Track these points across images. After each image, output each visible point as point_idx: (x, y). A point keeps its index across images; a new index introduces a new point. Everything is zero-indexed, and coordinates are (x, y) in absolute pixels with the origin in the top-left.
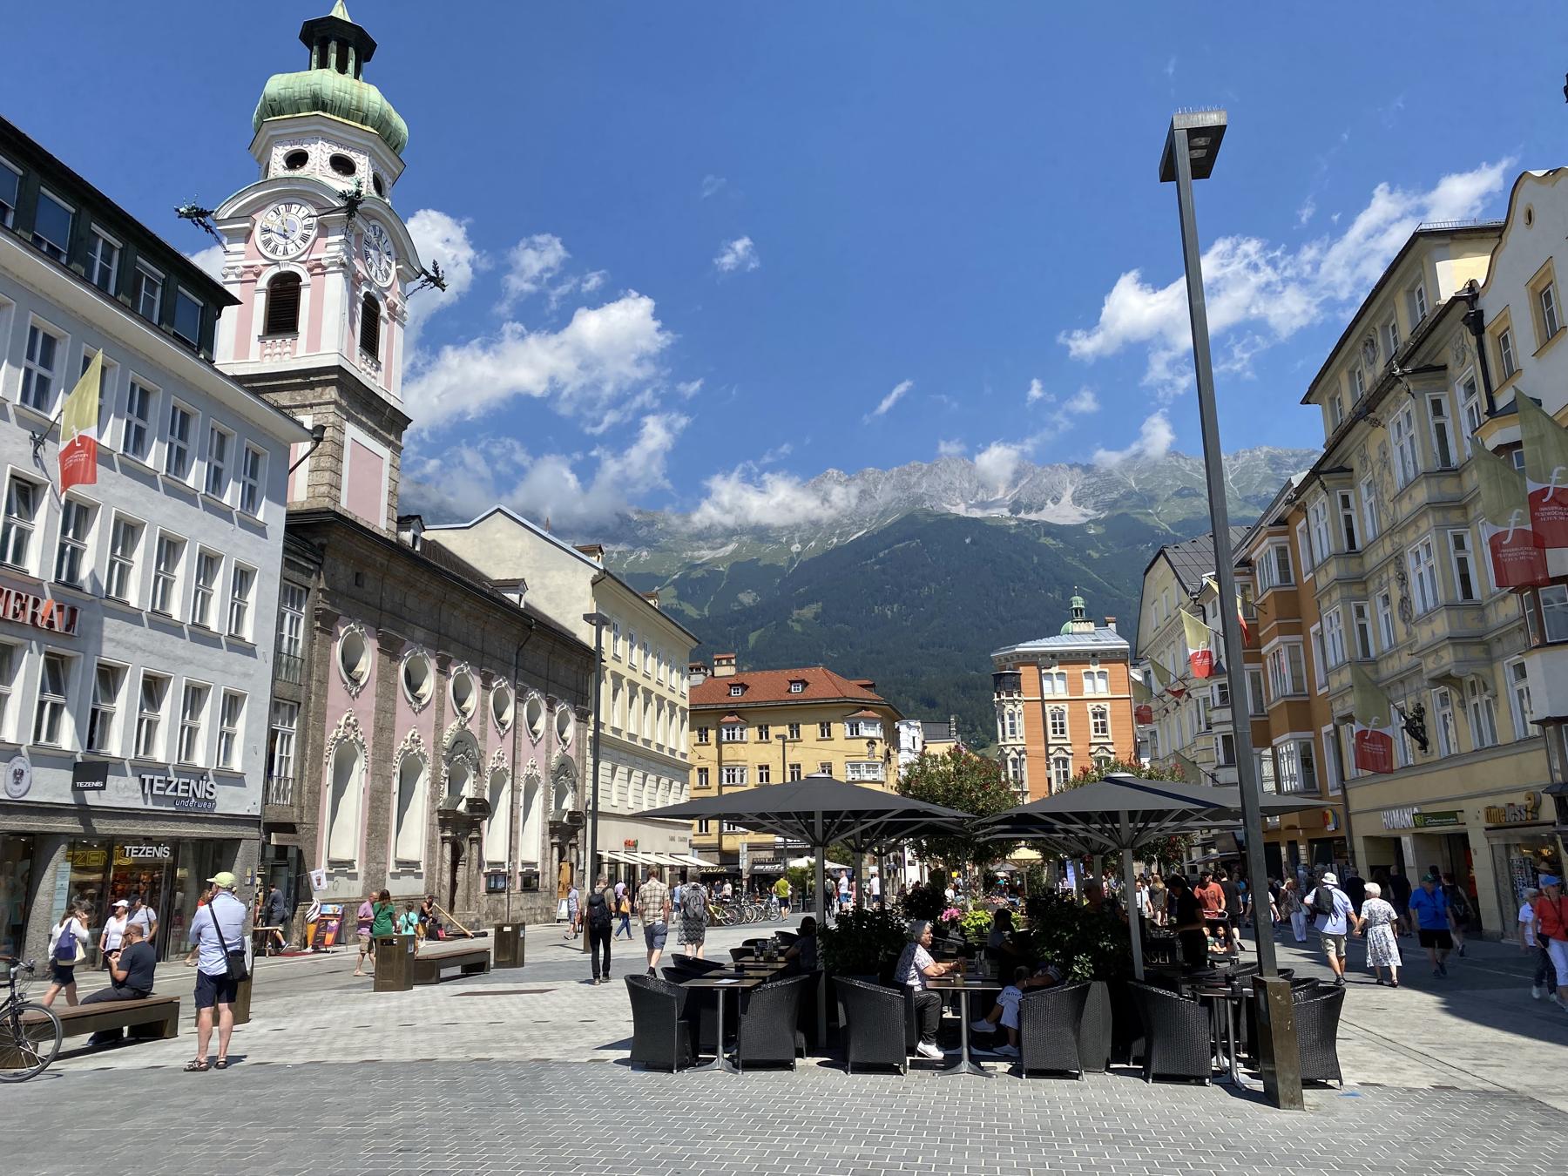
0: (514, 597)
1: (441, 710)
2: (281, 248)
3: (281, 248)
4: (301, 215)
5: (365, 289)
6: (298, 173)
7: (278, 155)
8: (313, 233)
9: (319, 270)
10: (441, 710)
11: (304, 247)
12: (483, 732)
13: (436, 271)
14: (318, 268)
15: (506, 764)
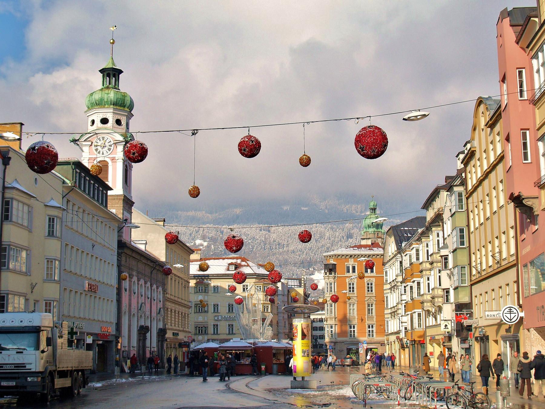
1: (138, 297)
2: (101, 152)
3: (101, 152)
4: (108, 141)
5: (125, 163)
6: (106, 126)
9: (114, 161)
10: (138, 297)
11: (109, 152)
12: (145, 302)
14: (113, 159)
15: (149, 313)
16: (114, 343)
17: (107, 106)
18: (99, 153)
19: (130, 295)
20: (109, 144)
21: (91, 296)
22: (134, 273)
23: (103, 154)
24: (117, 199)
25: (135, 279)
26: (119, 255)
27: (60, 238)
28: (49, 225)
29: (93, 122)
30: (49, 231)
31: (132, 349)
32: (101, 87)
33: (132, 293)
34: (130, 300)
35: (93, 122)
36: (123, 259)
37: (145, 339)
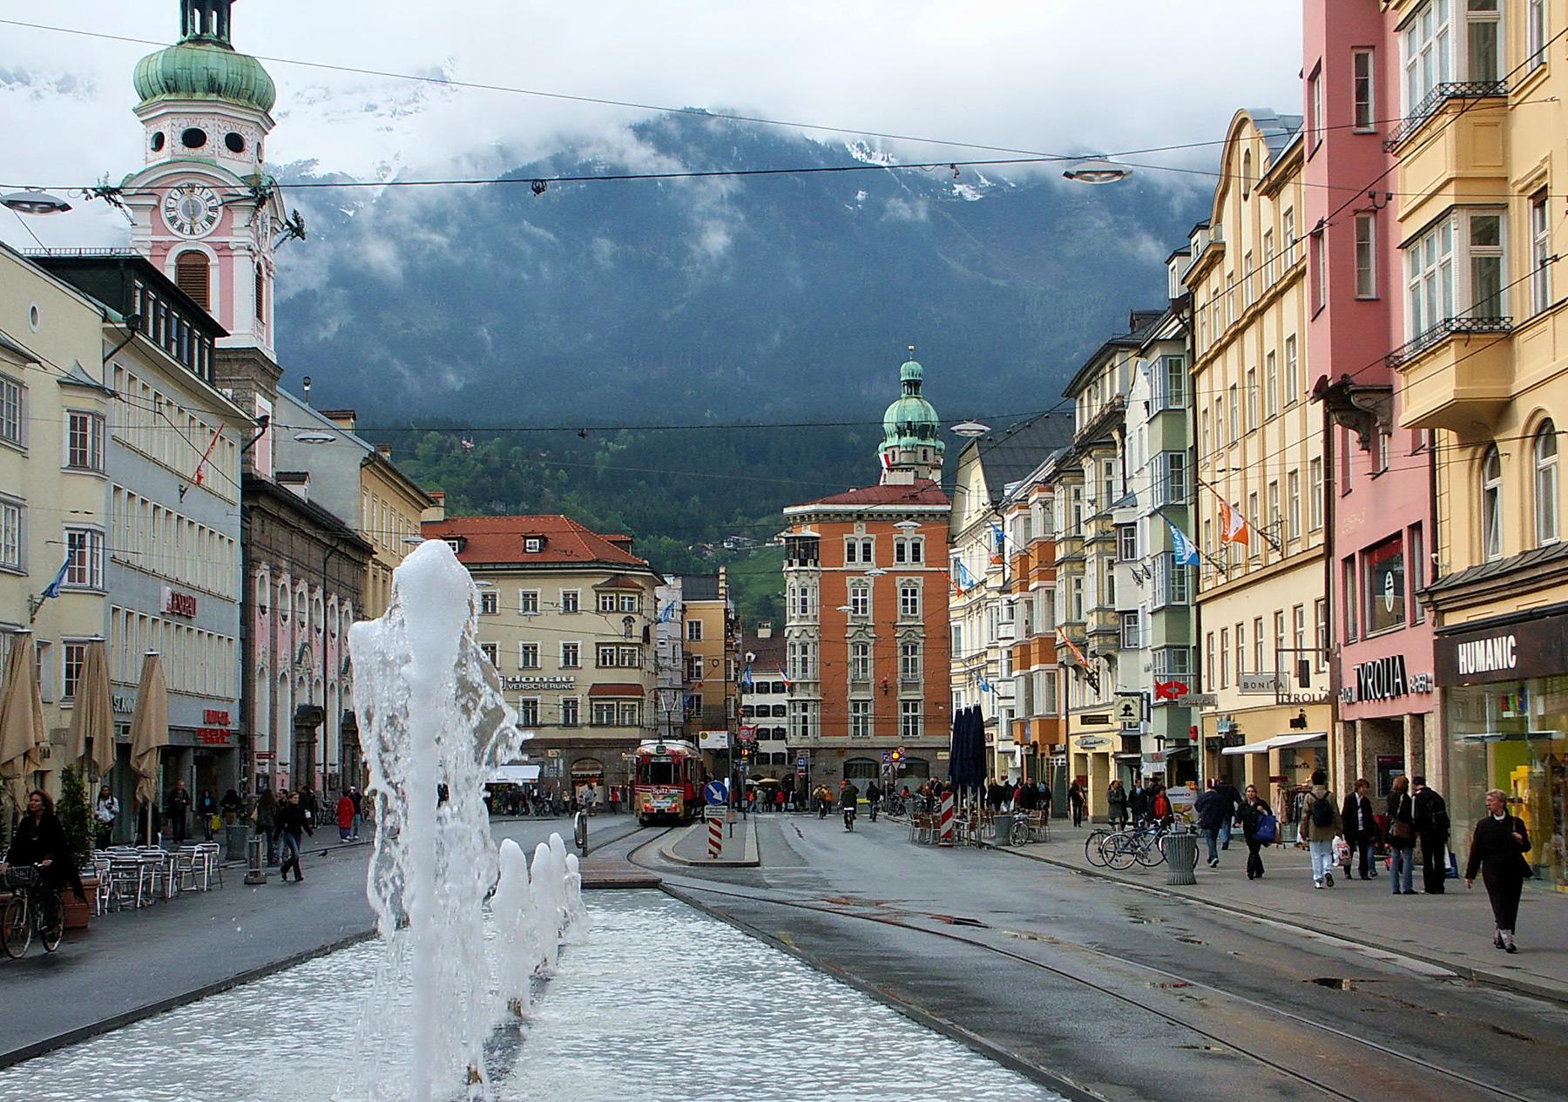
0: (298, 490)
2: (187, 227)
3: (187, 227)
6: (198, 152)
7: (173, 131)
8: (219, 216)
13: (297, 220)
14: (224, 249)
16: (237, 753)
17: (199, 95)
18: (181, 228)
19: (274, 625)
20: (210, 204)
21: (178, 627)
22: (284, 564)
23: (192, 232)
24: (236, 360)
25: (285, 579)
26: (246, 514)
27: (101, 476)
28: (73, 436)
29: (159, 141)
30: (73, 453)
31: (279, 769)
32: (178, 37)
33: (279, 617)
34: (274, 637)
35: (159, 141)
36: (256, 522)
37: (312, 742)
